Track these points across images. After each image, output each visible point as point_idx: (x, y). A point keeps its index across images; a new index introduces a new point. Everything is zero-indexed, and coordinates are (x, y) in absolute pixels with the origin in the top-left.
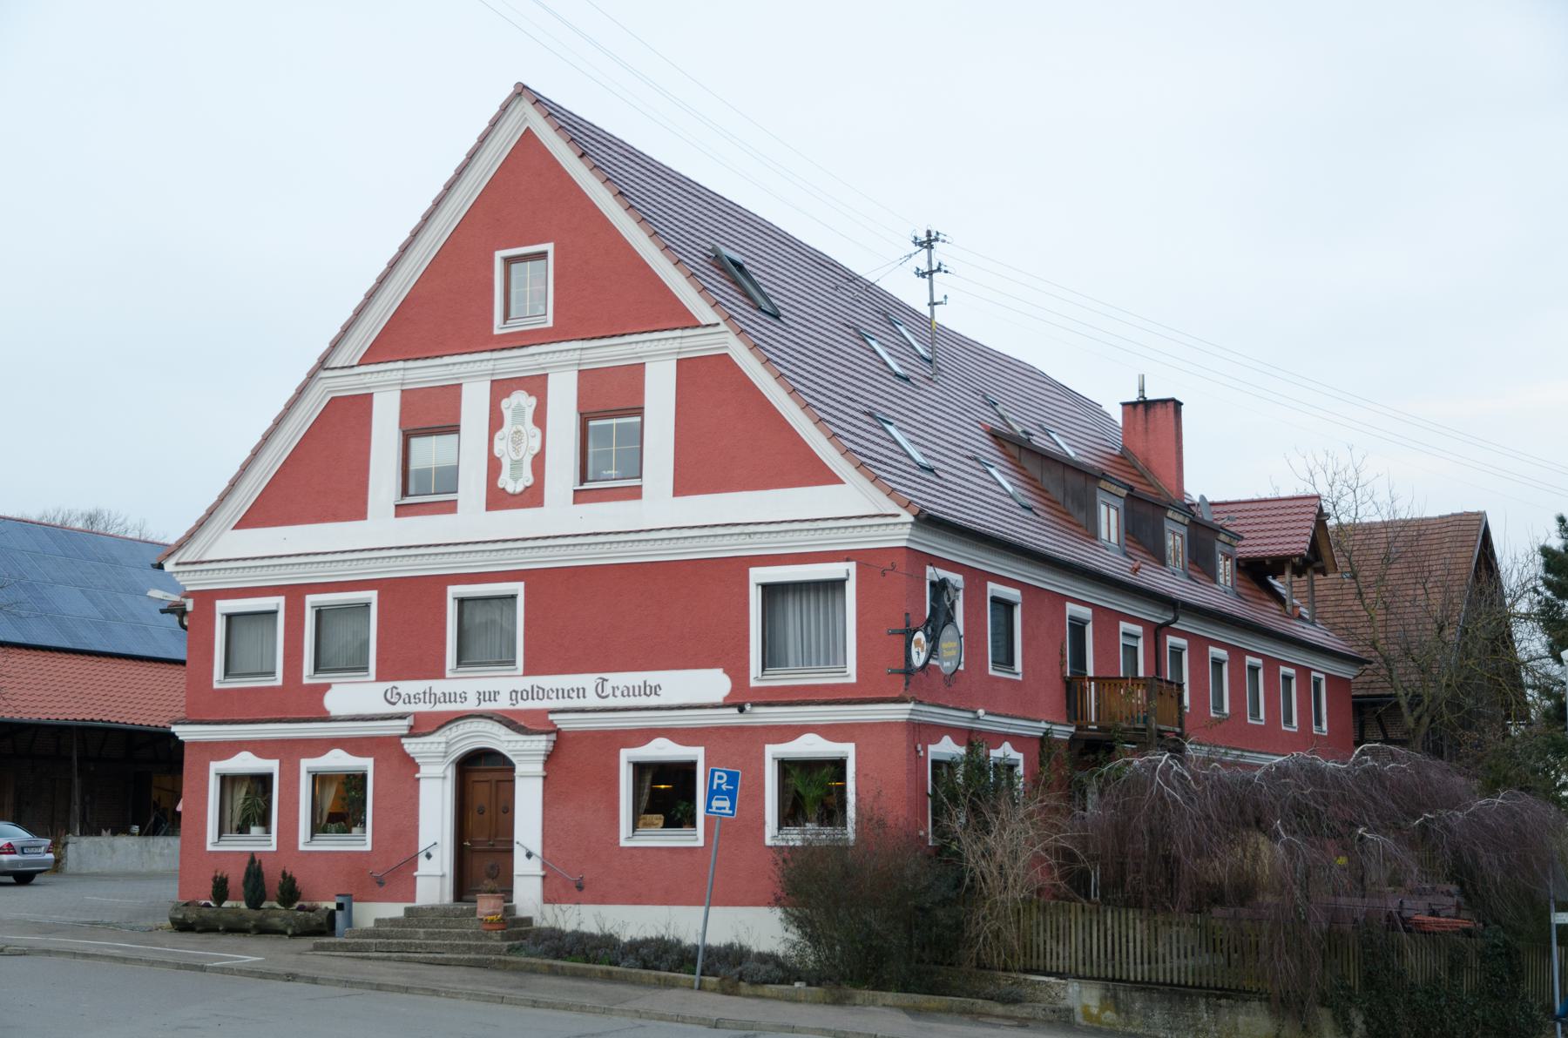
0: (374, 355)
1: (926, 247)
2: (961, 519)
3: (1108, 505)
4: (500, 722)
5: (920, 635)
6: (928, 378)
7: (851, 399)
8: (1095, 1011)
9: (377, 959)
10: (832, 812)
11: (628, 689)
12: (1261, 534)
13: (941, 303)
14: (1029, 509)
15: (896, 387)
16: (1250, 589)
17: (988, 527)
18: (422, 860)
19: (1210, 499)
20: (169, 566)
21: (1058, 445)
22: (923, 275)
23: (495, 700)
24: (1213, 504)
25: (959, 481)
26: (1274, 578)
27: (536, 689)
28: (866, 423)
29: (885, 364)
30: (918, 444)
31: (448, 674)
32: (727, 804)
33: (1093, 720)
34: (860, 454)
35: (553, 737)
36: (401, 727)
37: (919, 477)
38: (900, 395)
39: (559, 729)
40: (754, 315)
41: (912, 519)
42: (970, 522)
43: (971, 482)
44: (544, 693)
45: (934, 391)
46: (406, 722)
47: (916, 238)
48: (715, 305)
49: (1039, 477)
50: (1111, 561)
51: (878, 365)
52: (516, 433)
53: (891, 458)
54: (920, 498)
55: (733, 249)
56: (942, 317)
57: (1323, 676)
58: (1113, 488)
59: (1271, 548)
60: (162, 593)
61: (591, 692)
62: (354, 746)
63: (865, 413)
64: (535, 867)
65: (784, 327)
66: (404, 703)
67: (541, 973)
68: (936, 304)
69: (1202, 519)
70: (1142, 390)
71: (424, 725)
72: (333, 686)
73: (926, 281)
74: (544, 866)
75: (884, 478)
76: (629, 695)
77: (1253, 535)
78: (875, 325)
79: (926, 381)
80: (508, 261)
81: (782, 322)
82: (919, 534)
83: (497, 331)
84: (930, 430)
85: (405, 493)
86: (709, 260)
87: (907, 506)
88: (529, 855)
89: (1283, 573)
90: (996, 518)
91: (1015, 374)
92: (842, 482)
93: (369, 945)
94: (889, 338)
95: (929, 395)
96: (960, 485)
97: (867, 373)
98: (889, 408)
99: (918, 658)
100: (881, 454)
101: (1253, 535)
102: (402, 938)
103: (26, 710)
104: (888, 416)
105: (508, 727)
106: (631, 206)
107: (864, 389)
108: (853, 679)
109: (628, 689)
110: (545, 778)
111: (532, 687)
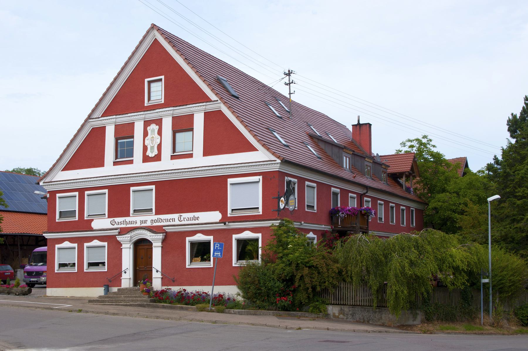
0: (106, 114)
1: (288, 75)
2: (297, 161)
3: (346, 157)
4: (147, 230)
5: (282, 199)
6: (288, 118)
7: (262, 124)
8: (337, 314)
9: (109, 305)
10: (253, 255)
11: (189, 218)
12: (396, 165)
13: (293, 93)
14: (320, 158)
15: (277, 120)
16: (392, 183)
17: (306, 164)
18: (123, 274)
19: (380, 155)
20: (41, 183)
21: (331, 138)
22: (287, 84)
23: (146, 223)
24: (381, 156)
25: (297, 150)
26: (400, 179)
27: (159, 219)
28: (267, 131)
29: (274, 113)
30: (284, 138)
31: (131, 215)
32: (219, 254)
33: (339, 224)
34: (264, 141)
35: (165, 234)
36: (116, 232)
37: (283, 148)
38: (278, 123)
39: (167, 232)
40: (230, 97)
41: (280, 161)
42: (300, 162)
43: (301, 150)
44: (161, 220)
45: (290, 122)
46: (117, 231)
47: (285, 73)
48: (216, 94)
49: (324, 148)
50: (347, 175)
51: (271, 113)
52: (152, 137)
53: (274, 143)
54: (283, 155)
55: (224, 77)
56: (294, 98)
57: (414, 209)
58: (348, 151)
59: (399, 169)
60: (39, 192)
61: (177, 220)
62: (101, 238)
63: (266, 128)
64: (159, 275)
65: (240, 101)
66: (117, 225)
67: (160, 308)
68: (291, 94)
69: (377, 161)
70: (359, 121)
71: (123, 231)
72: (94, 220)
73: (288, 86)
74: (162, 275)
75: (272, 149)
76: (189, 220)
77: (393, 166)
78: (271, 101)
79: (288, 118)
80: (150, 82)
81: (240, 100)
82: (283, 166)
83: (146, 105)
84: (288, 134)
85: (116, 158)
86: (216, 80)
87: (279, 157)
88: (157, 271)
89: (402, 177)
90: (309, 161)
91: (318, 116)
92: (258, 150)
93: (106, 300)
94: (276, 105)
95: (289, 123)
96: (297, 151)
97: (268, 116)
98: (275, 127)
99: (282, 206)
100: (271, 141)
101: (393, 166)
102: (116, 298)
103: (5, 230)
104: (274, 129)
105: (150, 231)
106: (189, 63)
107: (266, 121)
108: (261, 213)
109: (189, 218)
110: (162, 247)
111: (158, 218)
